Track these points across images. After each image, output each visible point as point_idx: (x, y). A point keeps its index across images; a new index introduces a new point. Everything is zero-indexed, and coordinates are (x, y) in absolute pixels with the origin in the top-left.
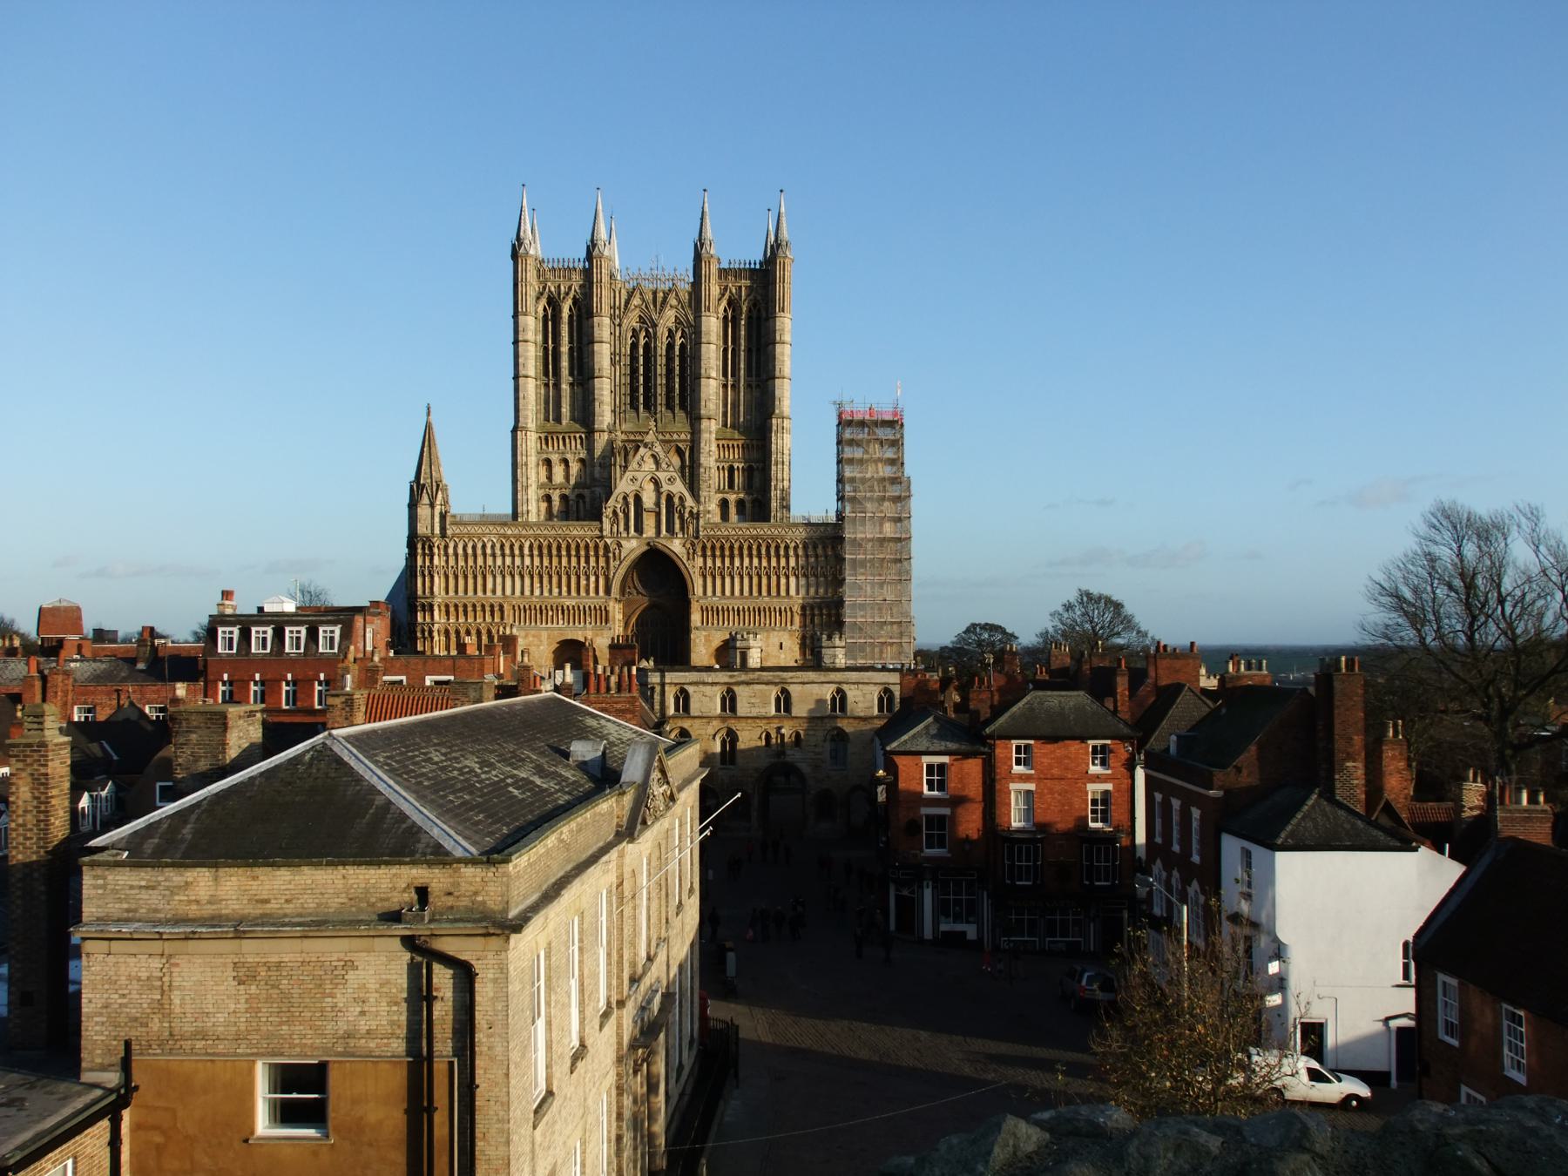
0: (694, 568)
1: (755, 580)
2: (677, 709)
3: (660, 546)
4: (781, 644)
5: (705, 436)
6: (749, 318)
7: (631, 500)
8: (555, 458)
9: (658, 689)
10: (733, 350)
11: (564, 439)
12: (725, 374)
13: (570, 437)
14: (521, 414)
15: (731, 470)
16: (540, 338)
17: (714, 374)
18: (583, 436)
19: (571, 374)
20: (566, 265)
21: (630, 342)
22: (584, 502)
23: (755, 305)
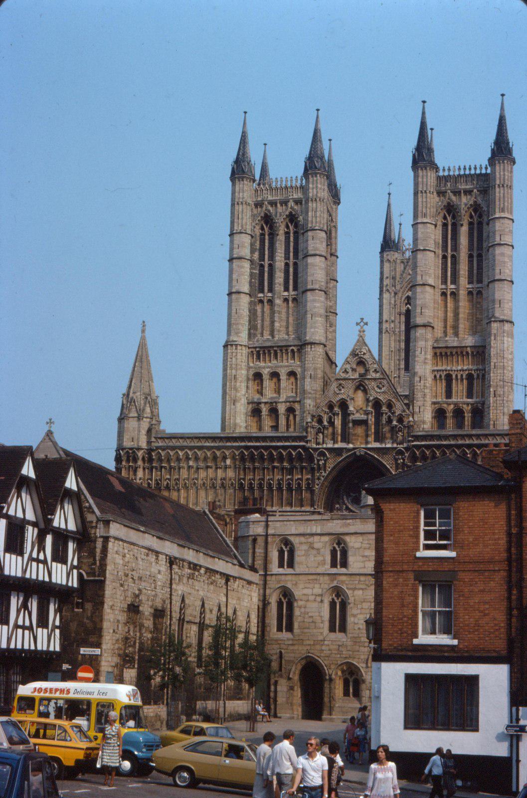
2: (281, 565)
8: (266, 372)
9: (260, 541)
10: (453, 257)
12: (444, 281)
13: (281, 350)
15: (449, 378)
16: (256, 255)
17: (431, 281)
19: (286, 289)
20: (284, 183)
21: (404, 309)
22: (295, 416)
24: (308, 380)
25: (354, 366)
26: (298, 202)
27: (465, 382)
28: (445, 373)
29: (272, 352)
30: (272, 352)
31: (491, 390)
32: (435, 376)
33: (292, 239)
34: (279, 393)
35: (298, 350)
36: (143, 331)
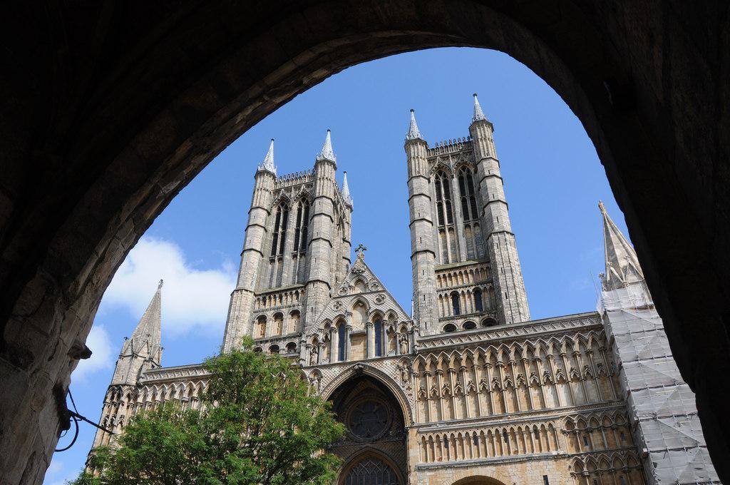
0: (410, 390)
1: (495, 397)
3: (367, 371)
4: (545, 478)
5: (422, 266)
6: (461, 180)
7: (334, 325)
8: (270, 314)
11: (281, 298)
13: (286, 294)
14: (242, 277)
15: (455, 296)
16: (271, 228)
18: (300, 291)
19: (296, 248)
23: (464, 169)
24: (309, 314)
25: (352, 284)
26: (308, 186)
27: (472, 296)
28: (451, 291)
29: (277, 295)
30: (277, 295)
31: (502, 292)
32: (441, 296)
33: (303, 211)
34: (281, 331)
35: (303, 291)
36: (160, 287)
